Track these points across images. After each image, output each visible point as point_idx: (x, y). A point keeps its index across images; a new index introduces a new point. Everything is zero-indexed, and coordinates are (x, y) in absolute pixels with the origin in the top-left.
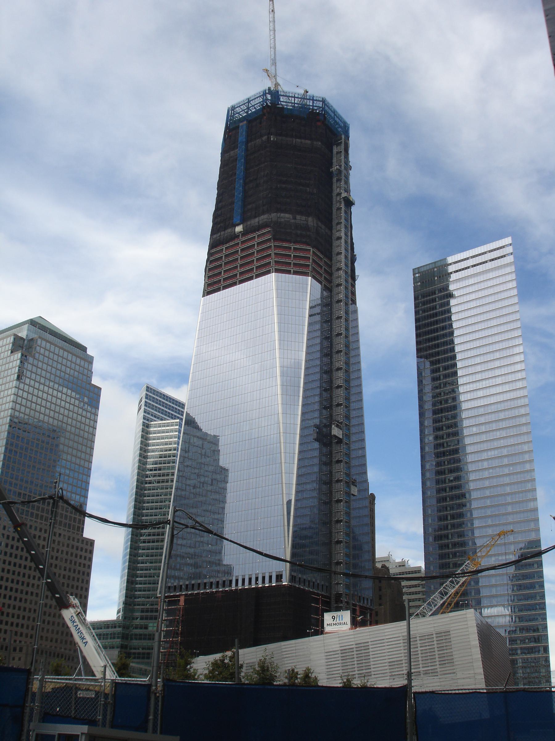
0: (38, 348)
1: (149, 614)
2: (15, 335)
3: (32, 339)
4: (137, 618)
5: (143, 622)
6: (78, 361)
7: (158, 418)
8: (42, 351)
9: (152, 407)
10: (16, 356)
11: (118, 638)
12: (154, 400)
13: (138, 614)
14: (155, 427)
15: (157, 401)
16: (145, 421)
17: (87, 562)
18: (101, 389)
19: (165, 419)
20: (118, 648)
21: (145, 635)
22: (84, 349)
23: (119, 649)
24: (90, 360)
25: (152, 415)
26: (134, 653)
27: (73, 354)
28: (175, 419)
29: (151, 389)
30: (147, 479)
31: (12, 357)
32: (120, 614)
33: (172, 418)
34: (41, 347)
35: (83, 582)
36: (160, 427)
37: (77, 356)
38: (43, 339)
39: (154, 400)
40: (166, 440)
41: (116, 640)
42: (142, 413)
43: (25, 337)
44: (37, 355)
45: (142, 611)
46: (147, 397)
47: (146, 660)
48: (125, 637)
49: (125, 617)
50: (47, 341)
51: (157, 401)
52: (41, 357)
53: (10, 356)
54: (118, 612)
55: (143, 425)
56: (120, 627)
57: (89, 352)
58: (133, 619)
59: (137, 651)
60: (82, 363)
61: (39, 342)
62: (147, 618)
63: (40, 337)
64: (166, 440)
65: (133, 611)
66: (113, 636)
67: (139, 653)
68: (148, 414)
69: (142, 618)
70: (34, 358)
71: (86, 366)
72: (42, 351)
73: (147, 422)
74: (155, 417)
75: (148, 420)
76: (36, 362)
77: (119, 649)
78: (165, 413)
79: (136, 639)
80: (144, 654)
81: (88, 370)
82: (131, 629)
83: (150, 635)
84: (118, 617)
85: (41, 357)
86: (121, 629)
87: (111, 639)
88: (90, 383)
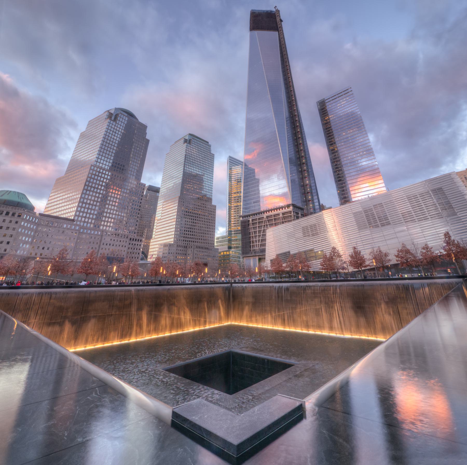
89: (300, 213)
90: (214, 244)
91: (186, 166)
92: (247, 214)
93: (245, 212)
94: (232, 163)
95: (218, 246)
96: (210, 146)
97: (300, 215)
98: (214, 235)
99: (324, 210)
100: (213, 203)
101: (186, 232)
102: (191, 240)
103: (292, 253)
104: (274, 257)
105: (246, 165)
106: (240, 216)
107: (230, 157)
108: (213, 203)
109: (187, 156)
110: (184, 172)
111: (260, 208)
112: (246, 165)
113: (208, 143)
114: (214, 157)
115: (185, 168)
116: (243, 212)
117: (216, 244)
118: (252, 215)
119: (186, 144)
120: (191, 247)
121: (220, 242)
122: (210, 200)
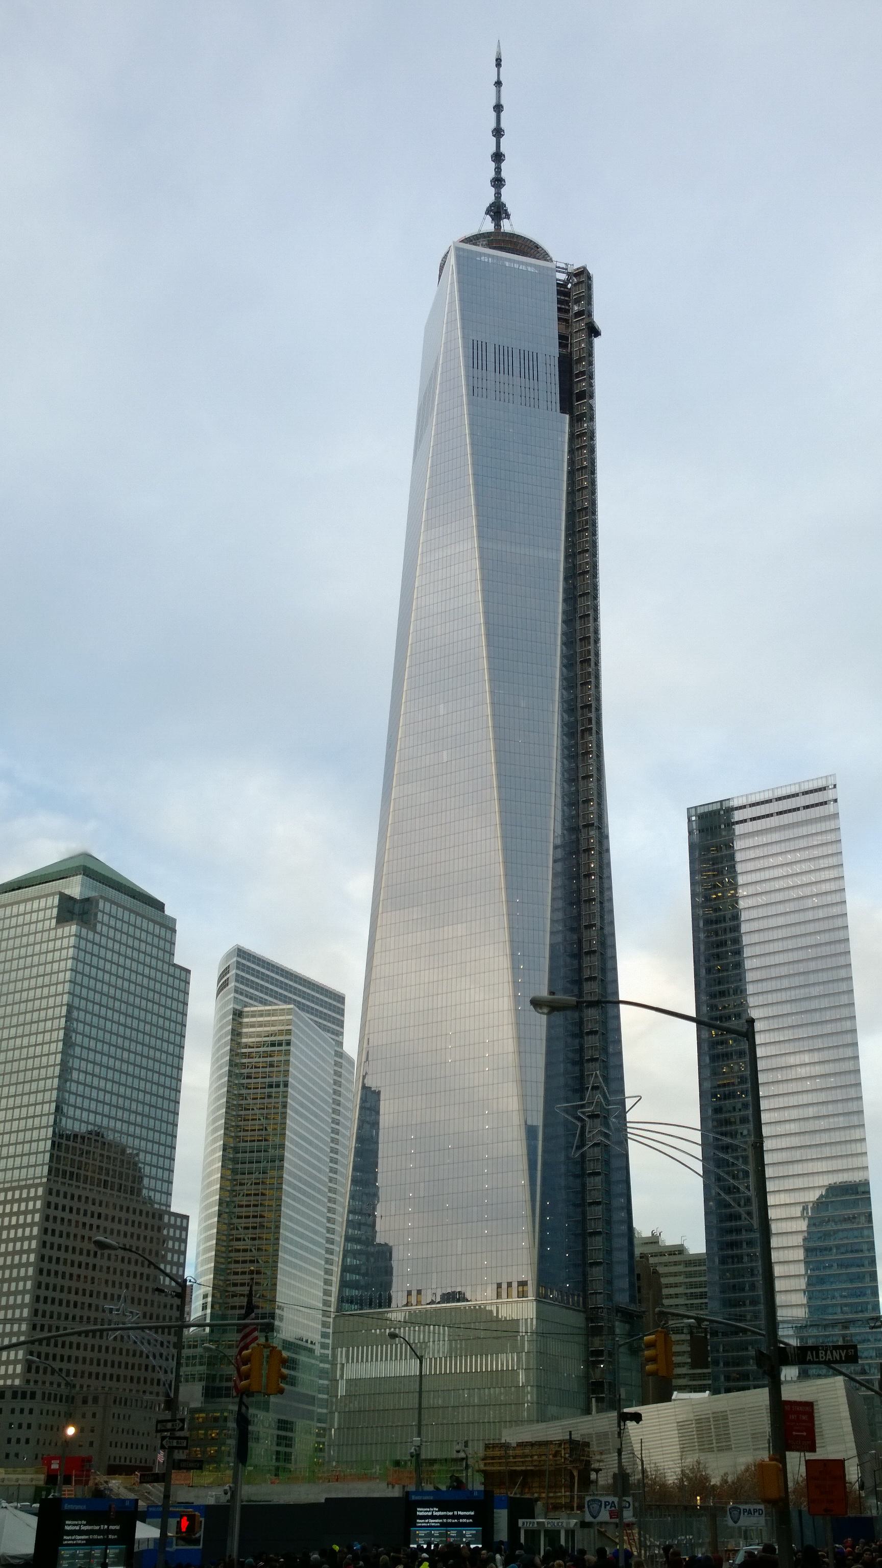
0: (100, 915)
3: (88, 900)
7: (261, 1002)
10: (67, 929)
19: (271, 1004)
22: (160, 906)
24: (169, 926)
25: (247, 996)
28: (289, 1003)
31: (60, 931)
33: (280, 1000)
34: (103, 912)
36: (261, 1016)
37: (150, 920)
38: (106, 899)
43: (77, 897)
44: (99, 926)
46: (239, 966)
50: (112, 902)
53: (55, 929)
55: (234, 1014)
57: (168, 911)
63: (102, 897)
68: (241, 994)
70: (95, 932)
72: (106, 918)
74: (256, 1000)
76: (97, 937)
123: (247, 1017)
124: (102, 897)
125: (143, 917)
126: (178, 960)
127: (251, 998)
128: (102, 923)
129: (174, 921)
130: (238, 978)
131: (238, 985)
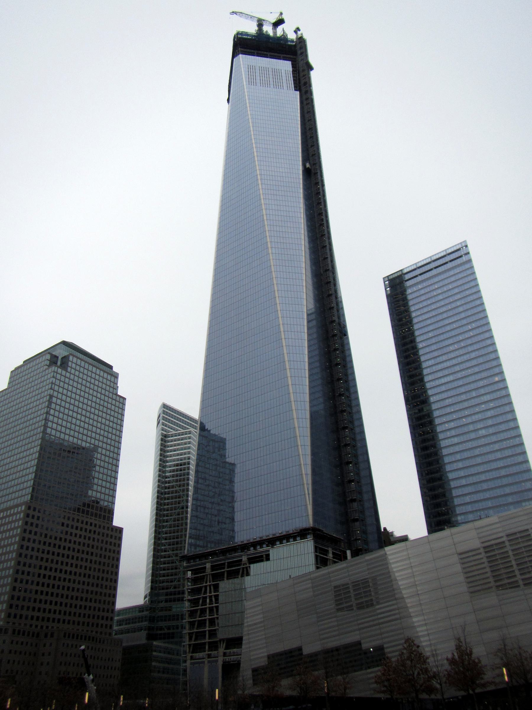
1: (172, 597)
2: (49, 353)
3: (65, 357)
4: (162, 602)
5: (168, 604)
6: (105, 375)
8: (74, 365)
9: (169, 421)
10: (50, 369)
11: (146, 621)
12: (170, 415)
13: (162, 598)
14: (172, 437)
15: (172, 416)
16: (163, 432)
17: (116, 549)
18: (124, 399)
20: (145, 630)
21: (170, 616)
23: (146, 632)
25: (169, 428)
26: (161, 634)
27: (101, 370)
29: (167, 406)
30: (167, 480)
31: (47, 371)
32: (147, 599)
34: (72, 362)
35: (112, 566)
39: (170, 415)
40: (182, 446)
41: (144, 623)
42: (160, 426)
45: (167, 594)
46: (164, 412)
47: (171, 640)
48: (152, 619)
49: (151, 601)
51: (172, 416)
52: (73, 371)
54: (145, 598)
56: (147, 610)
57: (114, 369)
58: (159, 602)
59: (163, 632)
60: (109, 377)
61: (71, 358)
62: (170, 601)
63: (71, 354)
64: (182, 446)
65: (158, 595)
66: (141, 619)
67: (165, 634)
68: (166, 426)
69: (166, 601)
70: (67, 371)
71: (113, 379)
73: (165, 433)
75: (166, 431)
77: (146, 632)
78: (180, 426)
79: (162, 621)
80: (169, 634)
81: (114, 383)
82: (157, 611)
83: (174, 616)
84: (145, 602)
85: (73, 371)
86: (147, 612)
87: (139, 622)
88: (116, 394)
89: (330, 551)
90: (111, 627)
91: (50, 424)
92: (200, 551)
93: (196, 546)
94: (169, 421)
95: (121, 632)
96: (116, 376)
97: (330, 555)
98: (114, 603)
99: (391, 543)
100: (116, 523)
101: (39, 597)
102: (52, 616)
103: (306, 651)
104: (263, 662)
105: (203, 428)
106: (185, 558)
107: (165, 406)
108: (116, 523)
109: (54, 400)
110: (43, 439)
111: (233, 537)
112: (203, 428)
113: (111, 367)
114: (124, 404)
115: (49, 430)
116: (190, 545)
117: (115, 628)
118: (213, 554)
119: (54, 368)
120: (52, 635)
121: (128, 621)
122: (109, 513)
123: (169, 437)
124: (71, 354)
125: (97, 368)
126: (120, 393)
127: (171, 429)
128: (71, 368)
129: (118, 374)
130: (164, 418)
131: (164, 421)
